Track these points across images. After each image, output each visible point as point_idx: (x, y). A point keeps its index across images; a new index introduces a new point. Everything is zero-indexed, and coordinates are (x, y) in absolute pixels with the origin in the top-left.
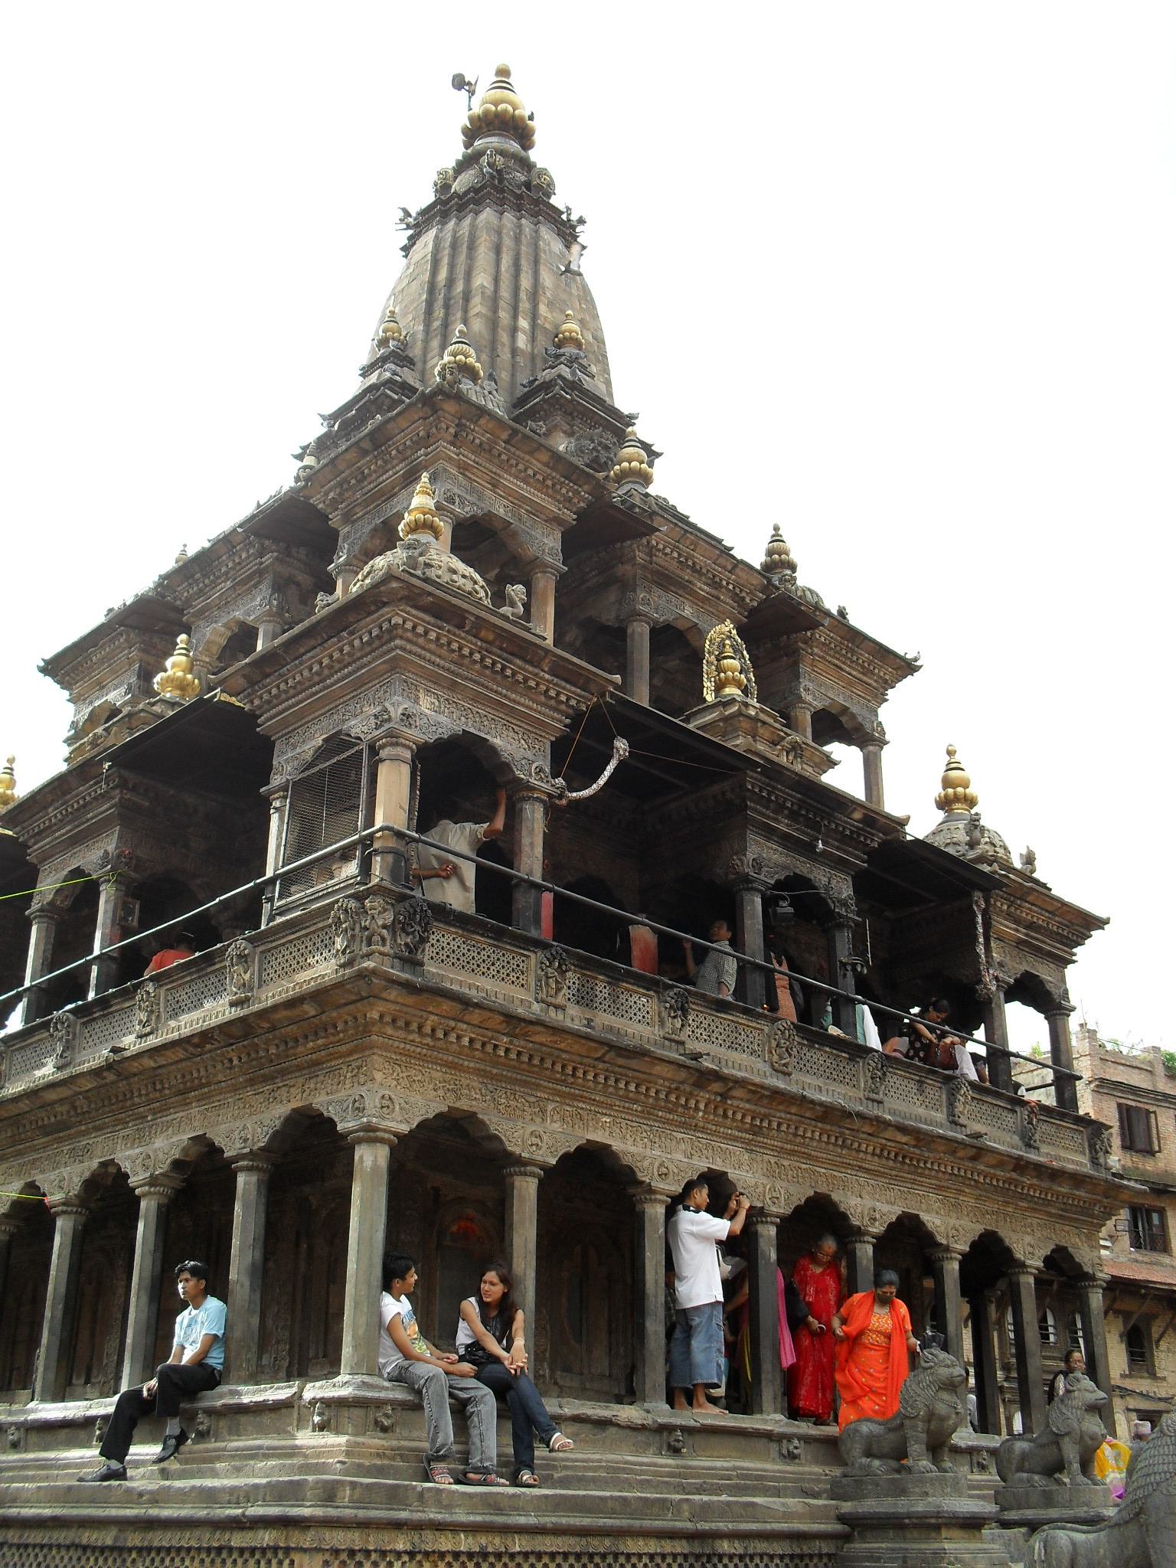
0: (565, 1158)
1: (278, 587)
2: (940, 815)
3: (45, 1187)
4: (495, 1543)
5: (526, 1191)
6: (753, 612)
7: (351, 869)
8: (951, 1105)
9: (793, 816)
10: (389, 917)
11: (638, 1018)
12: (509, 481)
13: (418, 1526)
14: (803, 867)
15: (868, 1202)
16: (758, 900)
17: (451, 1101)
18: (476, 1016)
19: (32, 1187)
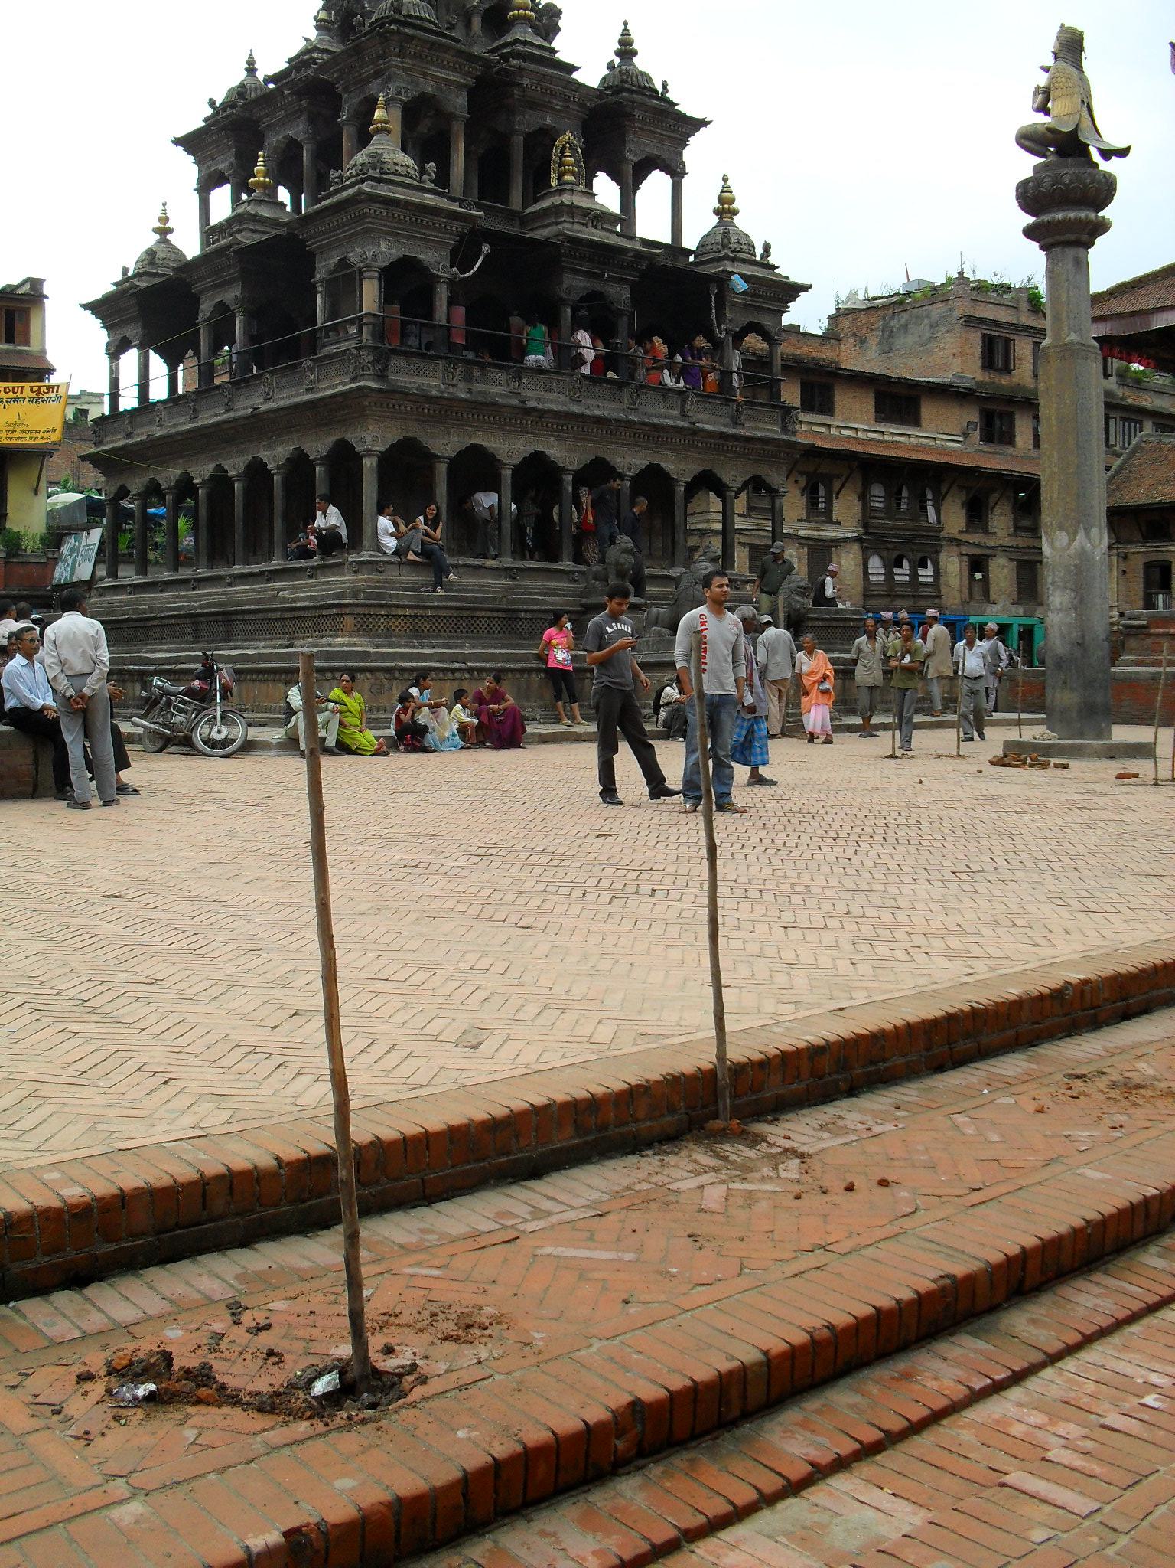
0: (460, 454)
1: (311, 120)
2: (716, 219)
3: (227, 468)
4: (420, 612)
5: (442, 469)
6: (591, 110)
7: (353, 330)
8: (683, 406)
9: (590, 260)
10: (371, 358)
11: (497, 386)
12: (434, 71)
13: (390, 606)
14: (598, 286)
15: (628, 460)
16: (569, 310)
17: (404, 434)
18: (413, 398)
19: (219, 467)
